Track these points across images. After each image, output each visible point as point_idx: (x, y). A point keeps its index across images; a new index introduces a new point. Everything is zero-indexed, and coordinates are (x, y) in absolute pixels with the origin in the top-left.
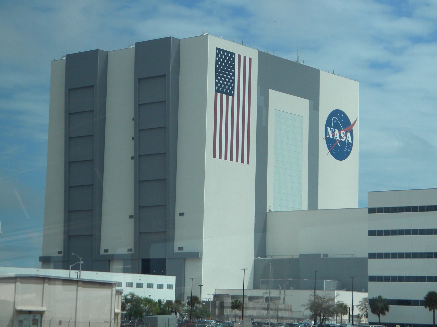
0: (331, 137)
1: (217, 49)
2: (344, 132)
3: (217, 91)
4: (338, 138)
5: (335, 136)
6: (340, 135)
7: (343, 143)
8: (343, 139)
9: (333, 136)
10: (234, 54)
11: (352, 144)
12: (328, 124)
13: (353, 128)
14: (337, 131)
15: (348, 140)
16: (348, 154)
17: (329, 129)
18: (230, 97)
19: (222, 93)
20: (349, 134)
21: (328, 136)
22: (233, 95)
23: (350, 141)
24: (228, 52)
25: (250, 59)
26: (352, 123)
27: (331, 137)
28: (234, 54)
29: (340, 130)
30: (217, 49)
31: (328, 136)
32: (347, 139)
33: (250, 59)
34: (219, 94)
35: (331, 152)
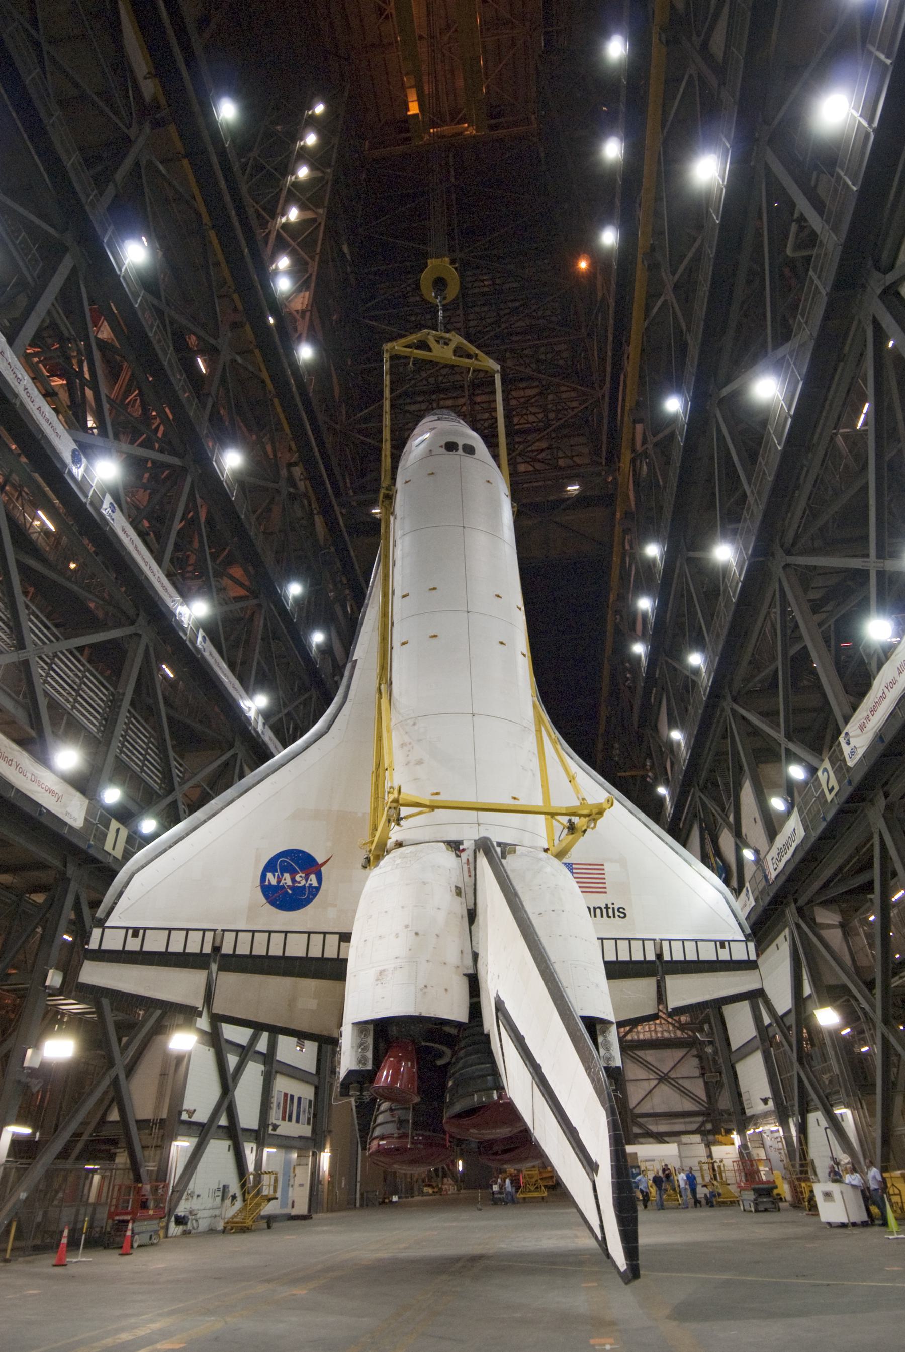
2: (303, 875)
4: (289, 883)
5: (283, 882)
6: (293, 880)
8: (299, 883)
9: (279, 882)
11: (318, 889)
14: (287, 876)
15: (311, 885)
16: (308, 901)
17: (269, 875)
20: (313, 877)
21: (267, 883)
23: (315, 883)
26: (320, 861)
27: (274, 882)
29: (293, 873)
31: (267, 883)
32: (309, 882)
35: (273, 903)
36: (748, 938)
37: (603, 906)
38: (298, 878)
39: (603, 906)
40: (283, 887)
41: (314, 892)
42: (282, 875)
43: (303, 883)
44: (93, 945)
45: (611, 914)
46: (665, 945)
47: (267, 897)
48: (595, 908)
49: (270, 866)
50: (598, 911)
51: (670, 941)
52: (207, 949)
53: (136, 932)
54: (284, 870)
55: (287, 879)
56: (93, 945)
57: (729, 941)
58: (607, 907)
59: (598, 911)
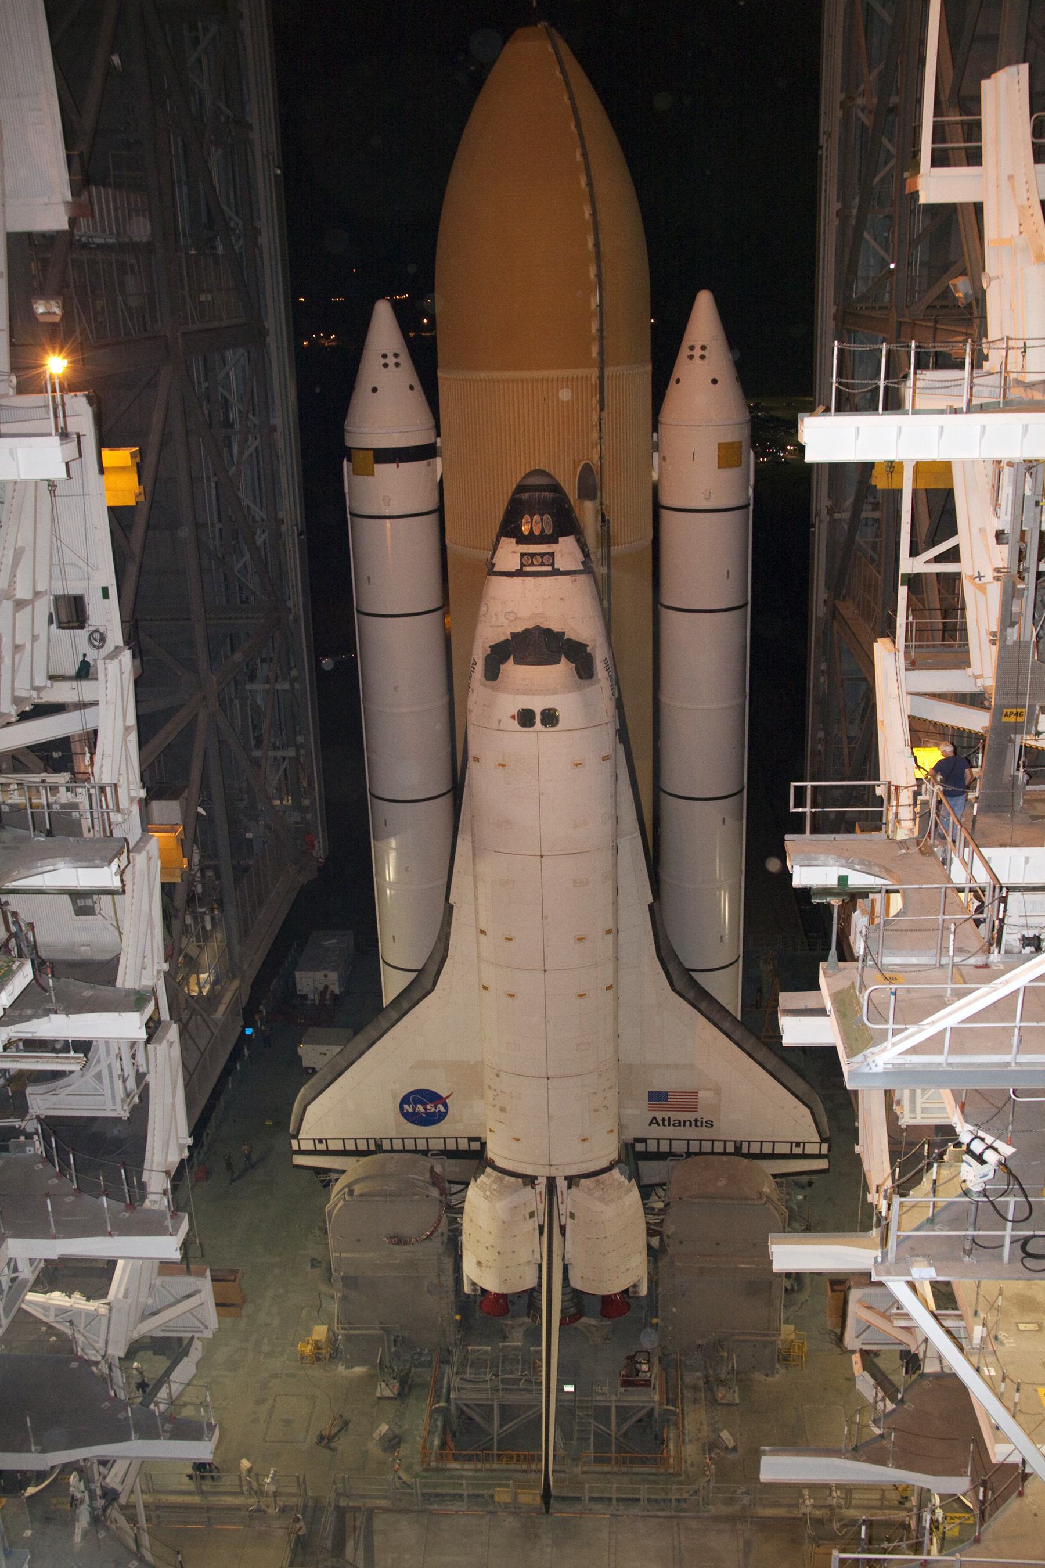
4: (422, 1110)
6: (425, 1109)
16: (439, 1121)
23: (443, 1109)
27: (410, 1110)
29: (424, 1104)
35: (413, 1122)
36: (823, 1140)
37: (692, 1119)
38: (428, 1107)
39: (692, 1119)
40: (418, 1113)
41: (442, 1116)
44: (295, 1147)
45: (699, 1124)
46: (745, 1145)
47: (408, 1120)
48: (685, 1122)
49: (405, 1100)
50: (688, 1123)
51: (749, 1142)
52: (373, 1148)
53: (320, 1141)
54: (416, 1102)
55: (420, 1108)
56: (295, 1147)
57: (804, 1143)
58: (696, 1120)
59: (688, 1123)
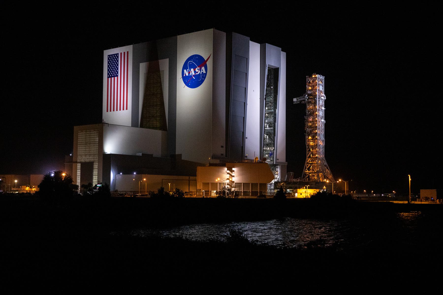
0: (187, 75)
1: (108, 56)
3: (108, 78)
4: (194, 74)
5: (191, 73)
7: (197, 76)
10: (118, 54)
11: (206, 74)
12: (185, 67)
13: (207, 63)
14: (192, 70)
15: (202, 72)
16: (202, 81)
17: (185, 71)
18: (116, 78)
19: (111, 77)
20: (203, 68)
22: (117, 76)
23: (204, 72)
24: (114, 55)
25: (128, 52)
26: (206, 60)
27: (187, 75)
28: (118, 54)
30: (108, 56)
33: (128, 52)
34: (110, 79)
38: (197, 70)
41: (204, 76)
42: (190, 70)
43: (199, 72)
